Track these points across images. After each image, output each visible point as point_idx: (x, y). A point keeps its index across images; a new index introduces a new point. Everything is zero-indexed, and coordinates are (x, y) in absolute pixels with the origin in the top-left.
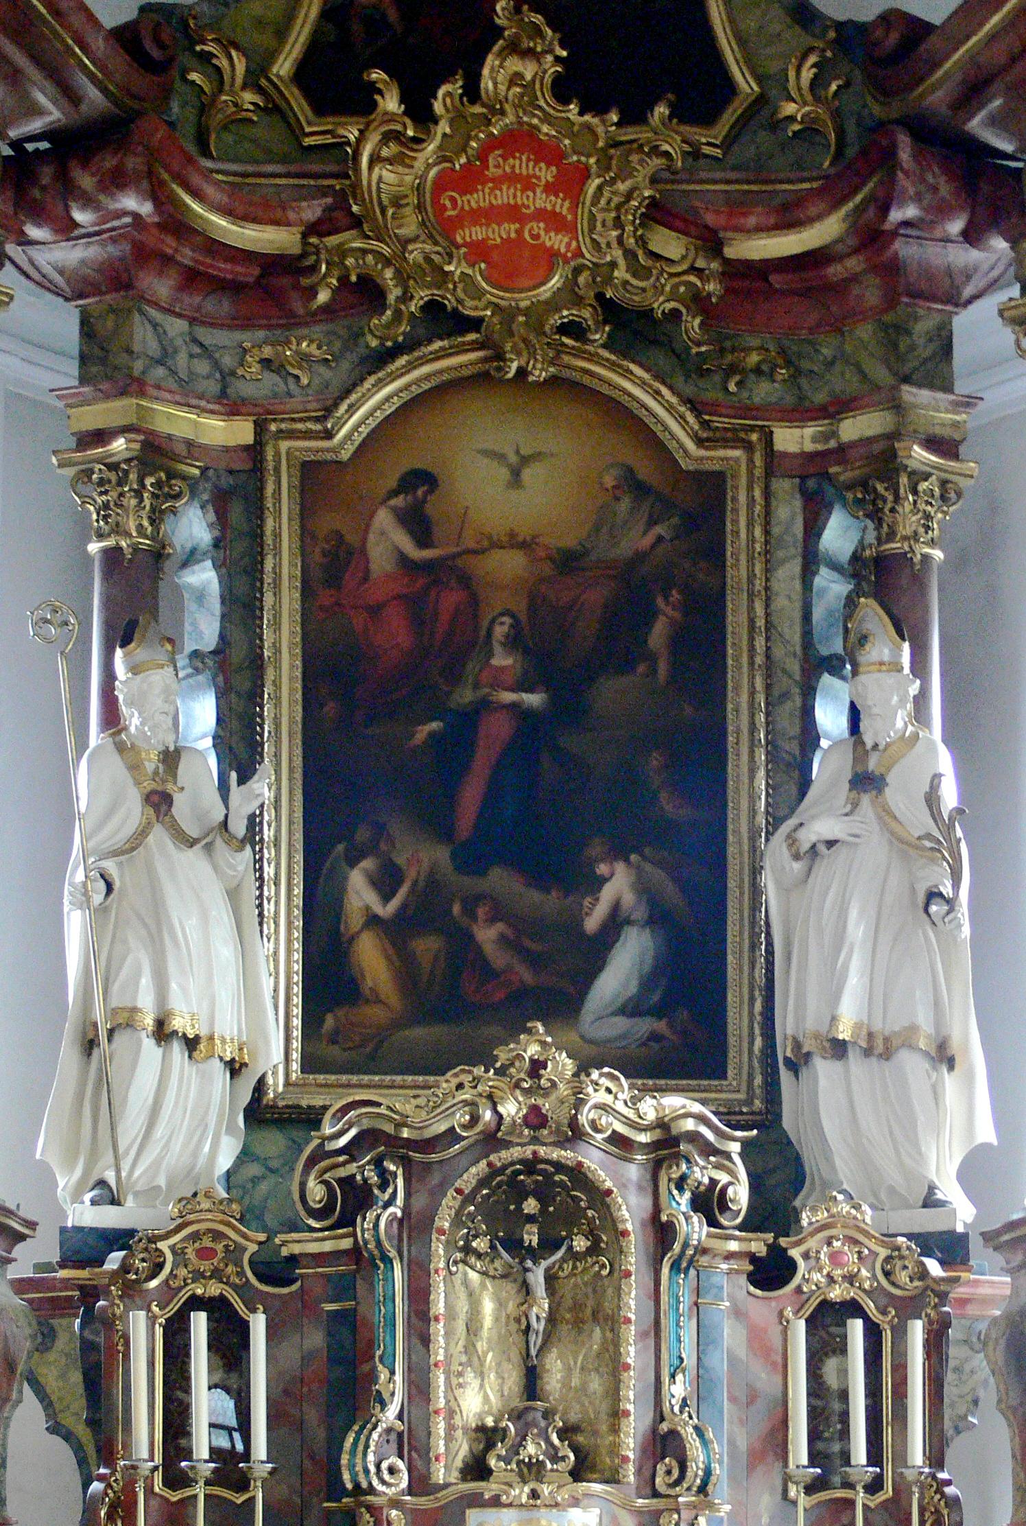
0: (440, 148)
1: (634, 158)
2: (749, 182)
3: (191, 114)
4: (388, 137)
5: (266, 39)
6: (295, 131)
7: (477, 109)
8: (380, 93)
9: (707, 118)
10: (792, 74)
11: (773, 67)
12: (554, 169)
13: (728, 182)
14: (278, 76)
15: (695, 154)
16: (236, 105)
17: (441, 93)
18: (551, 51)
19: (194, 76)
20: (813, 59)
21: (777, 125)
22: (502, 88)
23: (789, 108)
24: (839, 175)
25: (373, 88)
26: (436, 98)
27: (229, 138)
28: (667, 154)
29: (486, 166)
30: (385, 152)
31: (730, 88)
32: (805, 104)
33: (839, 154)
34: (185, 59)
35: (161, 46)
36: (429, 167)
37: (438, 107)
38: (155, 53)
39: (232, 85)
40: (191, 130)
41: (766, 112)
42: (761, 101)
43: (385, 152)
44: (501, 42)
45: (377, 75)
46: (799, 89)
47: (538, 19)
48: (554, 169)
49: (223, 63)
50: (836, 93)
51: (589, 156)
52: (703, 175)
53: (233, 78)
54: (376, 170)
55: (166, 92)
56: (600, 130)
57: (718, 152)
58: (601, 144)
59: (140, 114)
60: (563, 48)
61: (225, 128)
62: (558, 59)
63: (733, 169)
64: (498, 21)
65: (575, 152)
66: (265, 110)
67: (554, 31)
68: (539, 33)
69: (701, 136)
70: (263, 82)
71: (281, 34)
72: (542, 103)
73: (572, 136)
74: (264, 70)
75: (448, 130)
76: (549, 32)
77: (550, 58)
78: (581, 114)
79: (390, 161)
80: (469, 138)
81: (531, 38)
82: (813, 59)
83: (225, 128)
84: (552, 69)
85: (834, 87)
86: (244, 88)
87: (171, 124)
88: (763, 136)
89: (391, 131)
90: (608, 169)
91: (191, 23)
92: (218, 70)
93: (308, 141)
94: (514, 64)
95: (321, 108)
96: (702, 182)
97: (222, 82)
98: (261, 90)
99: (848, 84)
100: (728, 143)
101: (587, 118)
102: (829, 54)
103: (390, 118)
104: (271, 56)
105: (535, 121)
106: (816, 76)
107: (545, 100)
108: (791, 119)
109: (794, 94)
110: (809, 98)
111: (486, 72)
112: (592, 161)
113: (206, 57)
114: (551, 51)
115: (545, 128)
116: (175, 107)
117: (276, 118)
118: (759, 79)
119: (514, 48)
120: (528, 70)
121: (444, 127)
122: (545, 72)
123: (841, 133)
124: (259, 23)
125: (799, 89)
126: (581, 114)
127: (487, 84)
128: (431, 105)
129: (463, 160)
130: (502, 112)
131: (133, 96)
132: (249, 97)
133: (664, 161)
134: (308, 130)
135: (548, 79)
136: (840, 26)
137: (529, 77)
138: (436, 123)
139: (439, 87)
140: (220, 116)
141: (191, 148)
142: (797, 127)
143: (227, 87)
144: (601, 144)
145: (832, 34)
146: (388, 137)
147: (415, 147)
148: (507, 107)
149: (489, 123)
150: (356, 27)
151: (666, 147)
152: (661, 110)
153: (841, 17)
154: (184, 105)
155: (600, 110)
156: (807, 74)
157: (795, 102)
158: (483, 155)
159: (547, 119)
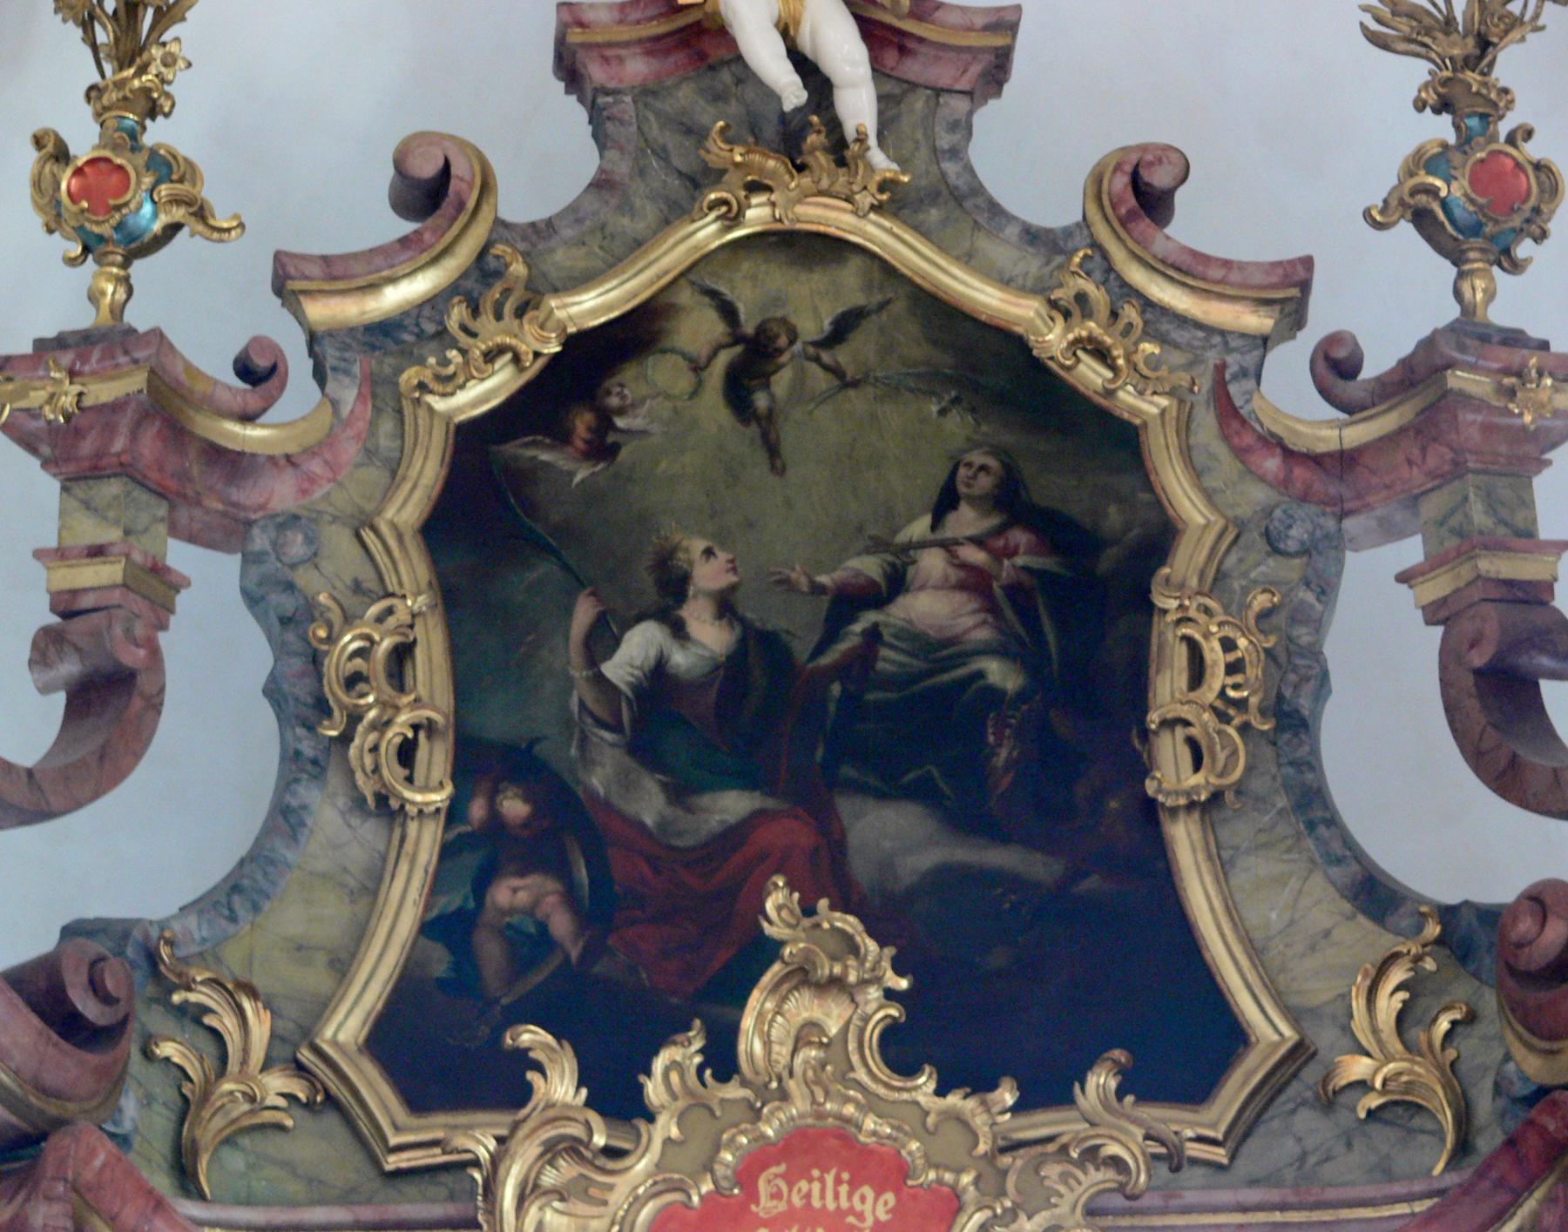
0: (660, 1166)
1: (1052, 1171)
2: (1283, 1207)
3: (160, 1122)
4: (551, 1152)
5: (316, 979)
6: (367, 1144)
7: (733, 1091)
8: (539, 1068)
9: (1197, 1092)
10: (1358, 1005)
11: (1319, 992)
12: (890, 1197)
13: (1244, 1209)
14: (334, 1043)
15: (1174, 1159)
16: (251, 1099)
17: (659, 1064)
18: (878, 980)
19: (167, 1049)
20: (1398, 975)
21: (1329, 1100)
22: (782, 1052)
23: (1358, 1068)
24: (1466, 1190)
25: (523, 1060)
26: (649, 1073)
27: (235, 1160)
28: (1116, 1162)
29: (752, 1195)
30: (549, 1178)
31: (1236, 1037)
32: (1389, 1058)
33: (1463, 1147)
34: (152, 1018)
35: (106, 999)
36: (637, 1202)
37: (654, 1090)
38: (90, 1009)
39: (244, 1062)
40: (160, 1146)
41: (1311, 1074)
42: (1300, 1054)
43: (549, 1178)
44: (776, 968)
45: (531, 1036)
46: (1375, 1031)
47: (849, 923)
48: (890, 1197)
49: (226, 1023)
50: (1448, 1035)
51: (959, 1171)
52: (1191, 1197)
53: (246, 1051)
54: (533, 1213)
55: (114, 1082)
56: (980, 1121)
57: (1220, 1155)
58: (982, 1148)
59: (60, 1123)
60: (899, 971)
61: (229, 1141)
62: (890, 995)
63: (1253, 1183)
64: (768, 929)
65: (931, 1164)
66: (309, 1106)
67: (882, 944)
68: (854, 949)
69: (1182, 1123)
70: (306, 1055)
71: (342, 966)
72: (861, 1075)
73: (924, 1133)
74: (307, 1034)
75: (674, 1132)
76: (872, 946)
77: (874, 993)
78: (941, 1091)
79: (561, 1194)
80: (717, 1147)
81: (834, 958)
82: (1398, 975)
83: (229, 1141)
84: (878, 1011)
85: (1443, 1025)
86: (265, 1067)
87: (123, 1141)
88: (1307, 1120)
89: (562, 1138)
90: (1002, 1193)
91: (165, 952)
92: (215, 1034)
93: (393, 1162)
94: (803, 1006)
95: (418, 1102)
96: (1186, 1210)
97: (223, 1058)
98: (301, 1069)
99: (1471, 1018)
100: (1241, 1133)
101: (954, 1099)
102: (1429, 965)
103: (561, 1114)
104: (322, 1008)
105: (849, 1110)
106: (1406, 1006)
107: (870, 1071)
108: (1363, 1086)
109: (1366, 1040)
110: (1396, 1046)
111: (748, 1022)
112: (966, 1179)
113: (194, 1014)
114: (878, 980)
115: (870, 1123)
116: (129, 1105)
117: (331, 1121)
118: (1294, 1015)
119: (802, 977)
120: (833, 1015)
121: (666, 1127)
122: (866, 1019)
123: (1464, 1118)
124: (300, 949)
125: (1375, 1031)
126: (941, 1091)
127: (750, 1044)
128: (640, 1089)
129: (707, 1187)
130: (784, 1096)
131: (44, 1091)
132: (276, 1084)
133: (1107, 1176)
134: (394, 1140)
135: (873, 1034)
136: (1447, 914)
137: (833, 1030)
138: (651, 1118)
139: (656, 1053)
140: (218, 1122)
141: (162, 1182)
142: (1374, 1101)
143: (233, 1065)
144: (982, 1148)
145: (1433, 930)
146: (551, 1152)
147: (611, 1165)
148: (792, 1085)
149: (756, 1115)
150: (491, 952)
151: (1113, 1149)
152: (1101, 1080)
153: (1450, 896)
154: (148, 1101)
155: (981, 1085)
156: (1389, 1004)
157: (1368, 1055)
158: (746, 1176)
159: (872, 1104)
